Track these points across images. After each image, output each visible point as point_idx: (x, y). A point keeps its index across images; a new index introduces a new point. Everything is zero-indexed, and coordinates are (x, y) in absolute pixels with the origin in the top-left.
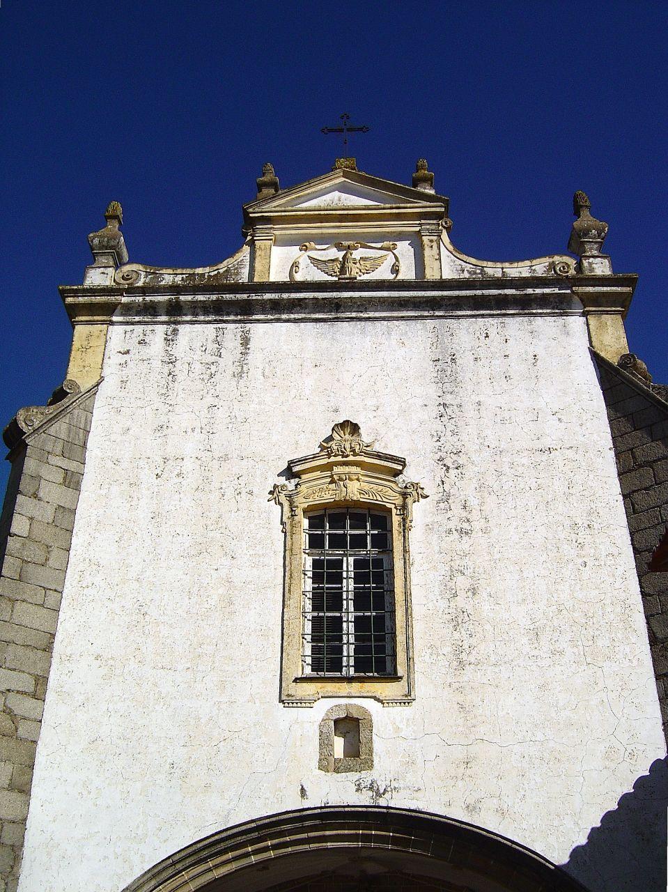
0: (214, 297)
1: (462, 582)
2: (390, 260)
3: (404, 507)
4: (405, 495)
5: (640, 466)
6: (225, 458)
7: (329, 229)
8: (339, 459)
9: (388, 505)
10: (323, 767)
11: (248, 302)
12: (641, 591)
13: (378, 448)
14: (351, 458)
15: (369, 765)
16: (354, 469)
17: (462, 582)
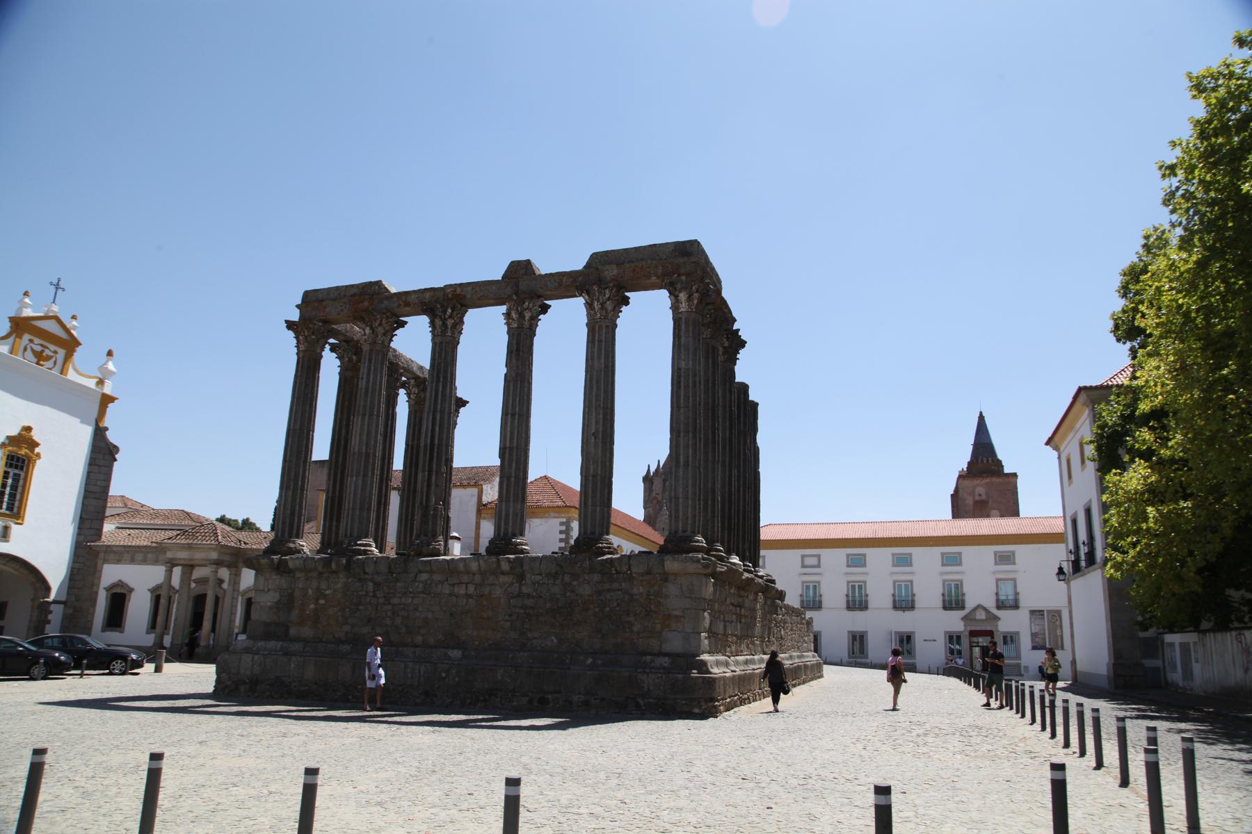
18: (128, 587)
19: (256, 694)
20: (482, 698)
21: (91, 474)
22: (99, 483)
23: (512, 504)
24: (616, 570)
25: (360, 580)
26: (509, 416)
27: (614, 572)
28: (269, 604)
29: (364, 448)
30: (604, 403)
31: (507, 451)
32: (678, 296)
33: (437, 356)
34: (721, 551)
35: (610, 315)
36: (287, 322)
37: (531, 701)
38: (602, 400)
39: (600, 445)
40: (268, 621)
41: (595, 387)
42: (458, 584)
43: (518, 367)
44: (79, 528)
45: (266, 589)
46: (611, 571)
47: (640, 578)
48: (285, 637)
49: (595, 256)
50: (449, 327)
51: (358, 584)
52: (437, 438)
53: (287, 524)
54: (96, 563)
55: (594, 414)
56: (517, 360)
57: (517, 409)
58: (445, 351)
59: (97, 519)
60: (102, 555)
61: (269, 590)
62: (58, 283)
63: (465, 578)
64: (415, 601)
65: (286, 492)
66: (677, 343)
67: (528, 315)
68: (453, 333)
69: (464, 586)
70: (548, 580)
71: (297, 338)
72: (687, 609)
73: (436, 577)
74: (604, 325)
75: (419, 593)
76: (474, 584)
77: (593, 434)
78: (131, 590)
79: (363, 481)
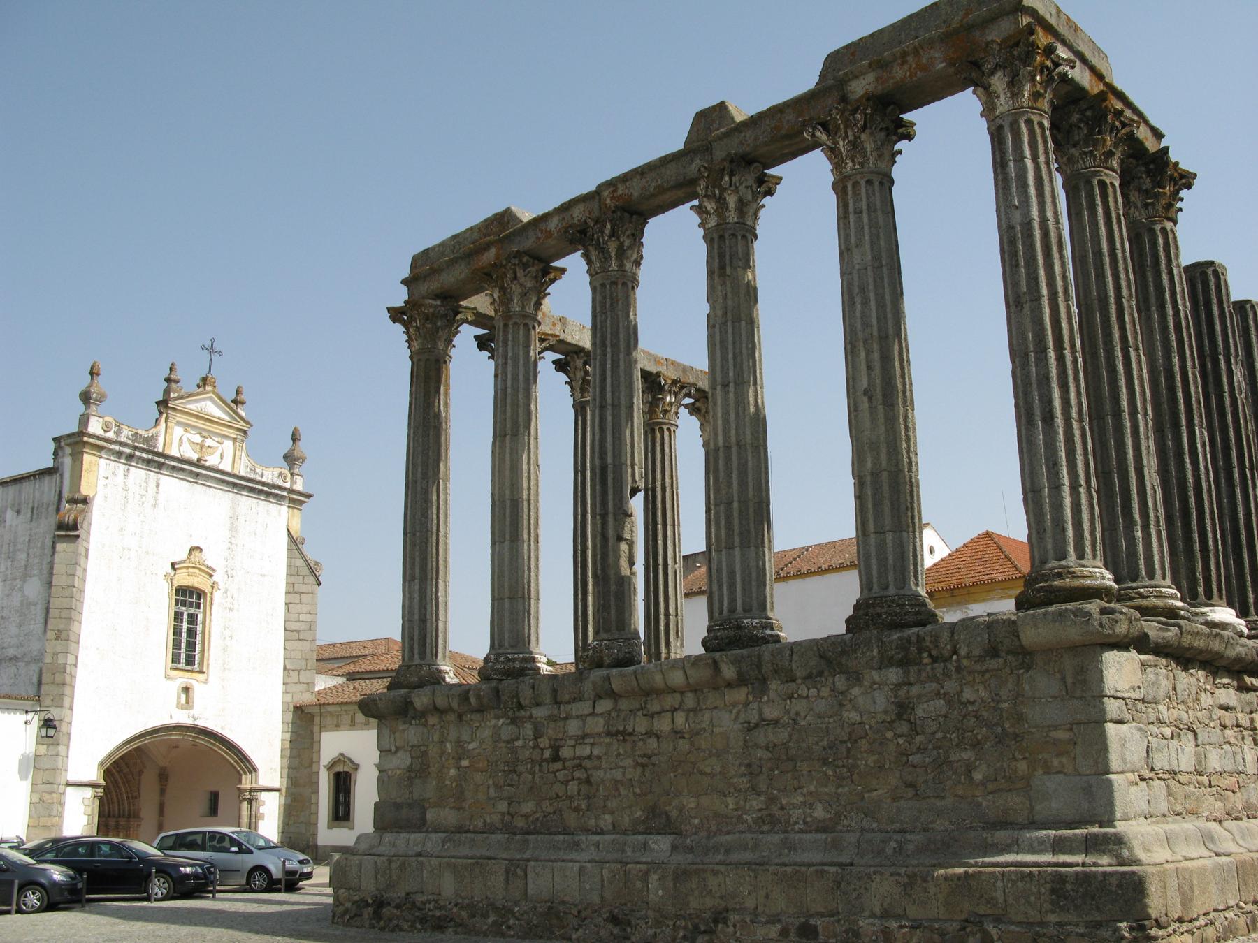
0: (150, 457)
1: (228, 633)
2: (219, 451)
3: (212, 593)
4: (213, 587)
6: (147, 553)
7: (200, 424)
10: (177, 707)
11: (163, 464)
13: (206, 563)
15: (192, 708)
16: (197, 571)
17: (228, 633)
18: (352, 762)
19: (382, 923)
20: (703, 928)
21: (291, 606)
22: (303, 617)
23: (737, 552)
24: (930, 656)
25: (514, 721)
26: (719, 387)
27: (926, 661)
28: (398, 772)
29: (508, 492)
30: (879, 330)
31: (721, 454)
32: (990, 85)
33: (598, 309)
34: (1173, 597)
35: (871, 160)
36: (389, 309)
37: (784, 933)
38: (875, 322)
39: (881, 408)
40: (398, 800)
41: (858, 300)
42: (659, 713)
43: (725, 297)
45: (393, 749)
46: (921, 658)
47: (978, 667)
48: (420, 825)
49: (834, 60)
50: (613, 254)
51: (513, 728)
52: (610, 454)
53: (416, 638)
54: (312, 732)
55: (863, 355)
56: (724, 283)
57: (731, 374)
58: (612, 299)
60: (317, 720)
61: (397, 749)
63: (670, 701)
64: (596, 752)
65: (410, 587)
66: (1000, 177)
67: (732, 200)
68: (621, 266)
69: (669, 714)
70: (809, 689)
71: (407, 333)
72: (1079, 724)
73: (624, 705)
74: (863, 182)
75: (599, 735)
76: (683, 711)
77: (866, 392)
79: (511, 548)
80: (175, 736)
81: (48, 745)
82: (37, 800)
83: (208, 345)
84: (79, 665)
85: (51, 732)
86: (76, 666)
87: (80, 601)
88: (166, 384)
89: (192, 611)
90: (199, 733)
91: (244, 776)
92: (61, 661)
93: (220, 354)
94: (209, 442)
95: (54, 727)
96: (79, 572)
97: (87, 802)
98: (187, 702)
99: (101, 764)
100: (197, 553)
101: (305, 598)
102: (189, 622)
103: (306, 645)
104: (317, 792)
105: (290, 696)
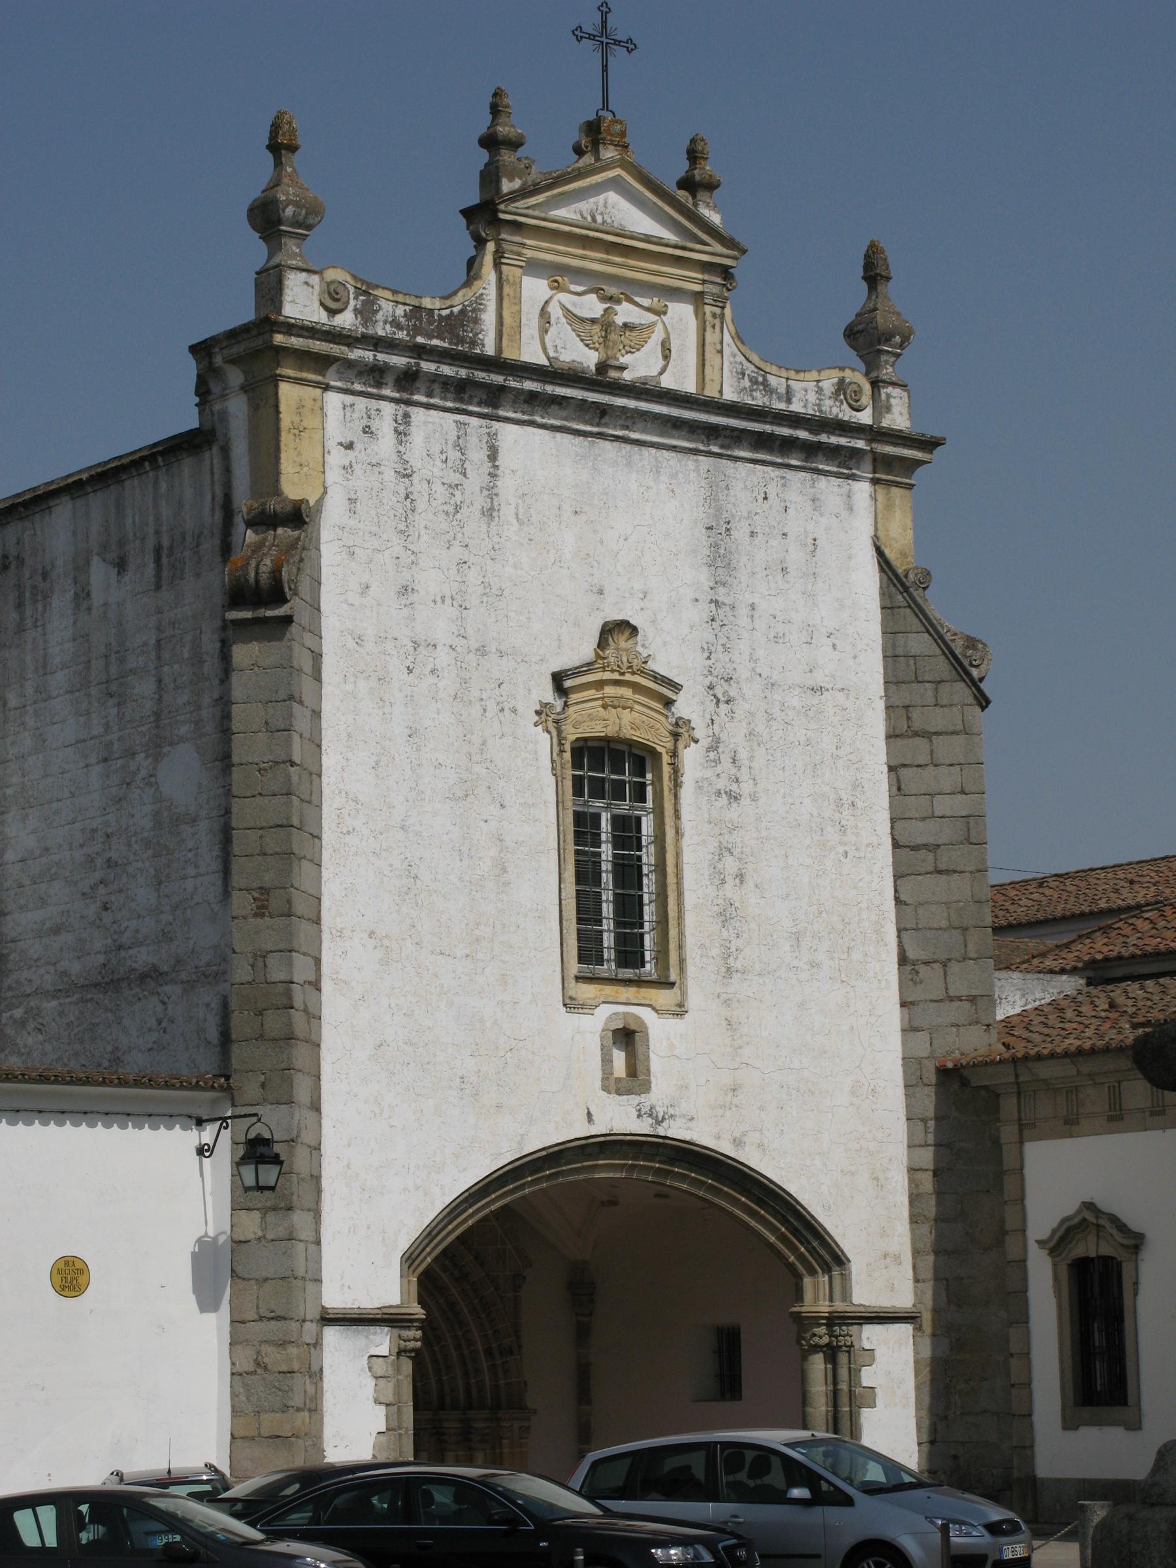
0: (463, 373)
1: (730, 865)
2: (657, 336)
3: (674, 754)
4: (676, 736)
5: (916, 734)
6: (482, 651)
7: (594, 261)
8: (616, 676)
9: (659, 749)
10: (605, 1088)
11: (502, 389)
12: (895, 896)
13: (652, 665)
14: (628, 677)
15: (645, 1087)
16: (627, 692)
17: (730, 865)
18: (1122, 1227)
21: (903, 772)
22: (944, 805)
44: (903, 1005)
54: (997, 1144)
59: (965, 958)
60: (1009, 1105)
62: (604, 23)
78: (1136, 1242)
80: (606, 1171)
81: (265, 1211)
82: (251, 1367)
83: (591, 22)
84: (326, 985)
85: (269, 1174)
86: (316, 985)
87: (314, 802)
88: (484, 156)
89: (624, 807)
90: (672, 1161)
91: (807, 1281)
92: (277, 975)
93: (630, 46)
94: (625, 313)
95: (276, 1160)
96: (301, 721)
97: (381, 1367)
98: (632, 1072)
99: (409, 1259)
100: (622, 641)
101: (948, 748)
102: (618, 842)
103: (959, 888)
104: (1022, 1318)
105: (923, 1037)
